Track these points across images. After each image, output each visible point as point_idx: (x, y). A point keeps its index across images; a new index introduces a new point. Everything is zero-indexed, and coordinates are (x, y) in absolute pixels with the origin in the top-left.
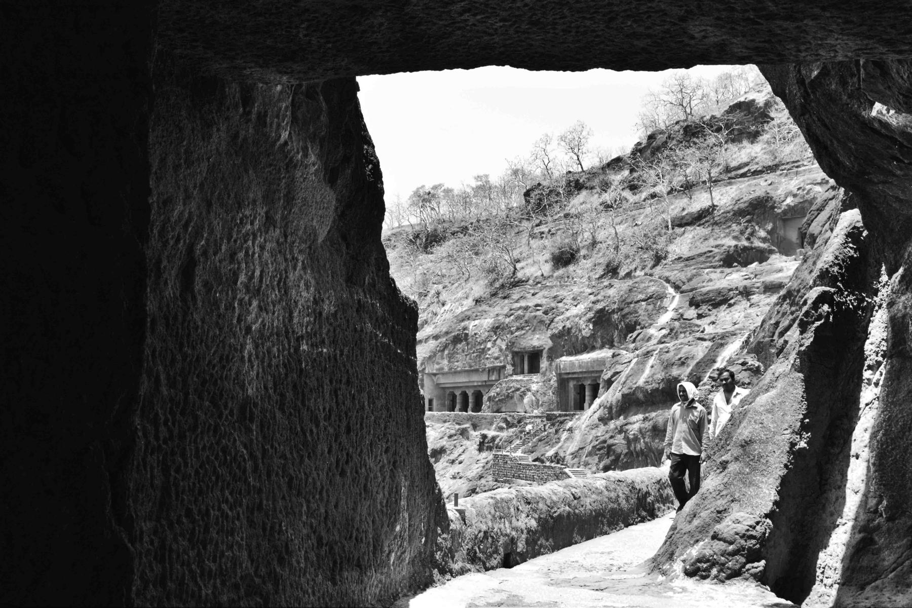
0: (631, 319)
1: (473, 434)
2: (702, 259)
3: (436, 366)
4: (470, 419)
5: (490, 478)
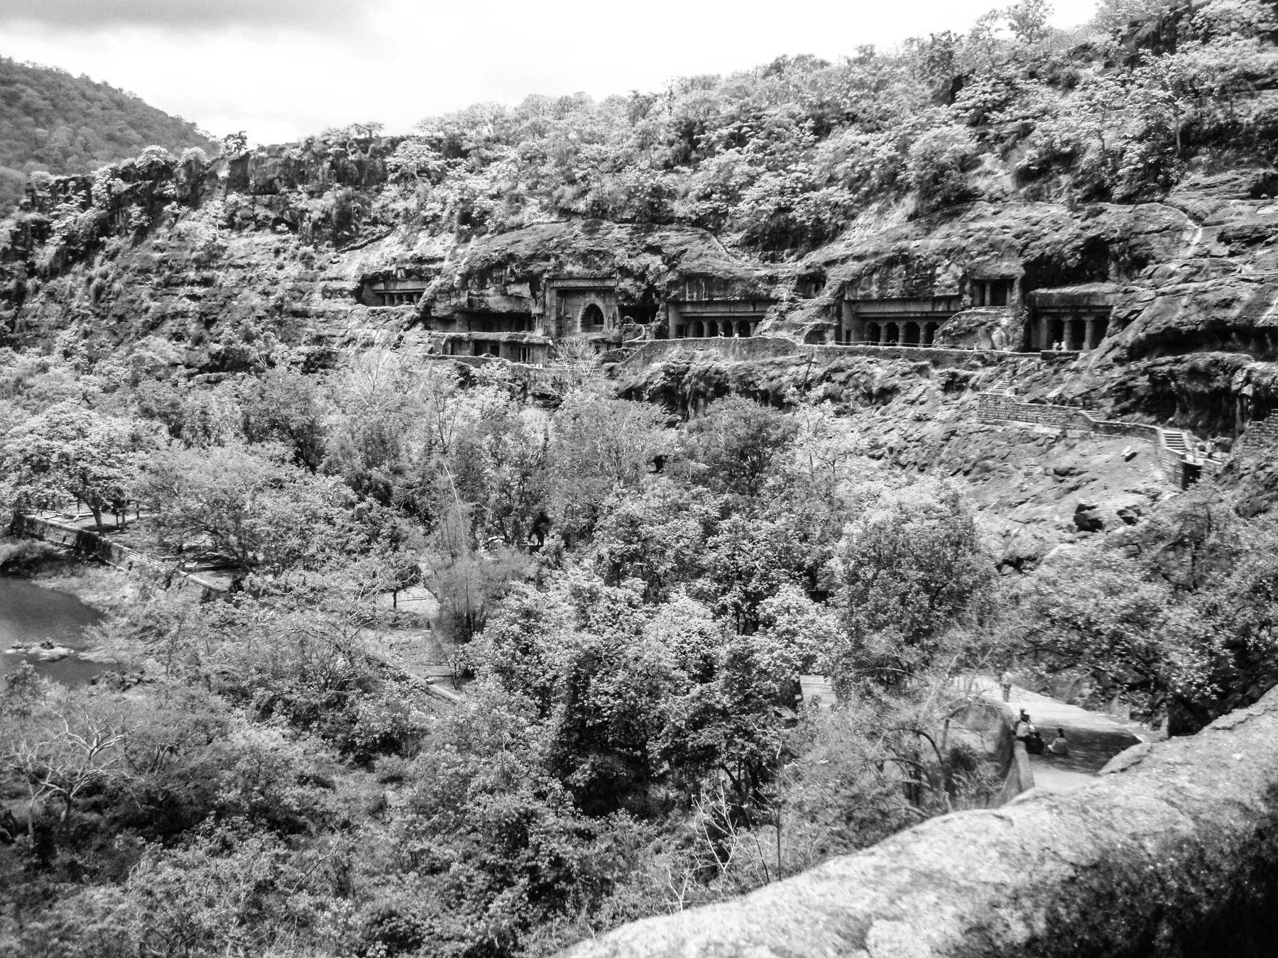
0: (1142, 251)
1: (935, 372)
2: (1225, 187)
3: (860, 293)
4: (928, 355)
5: (974, 420)
